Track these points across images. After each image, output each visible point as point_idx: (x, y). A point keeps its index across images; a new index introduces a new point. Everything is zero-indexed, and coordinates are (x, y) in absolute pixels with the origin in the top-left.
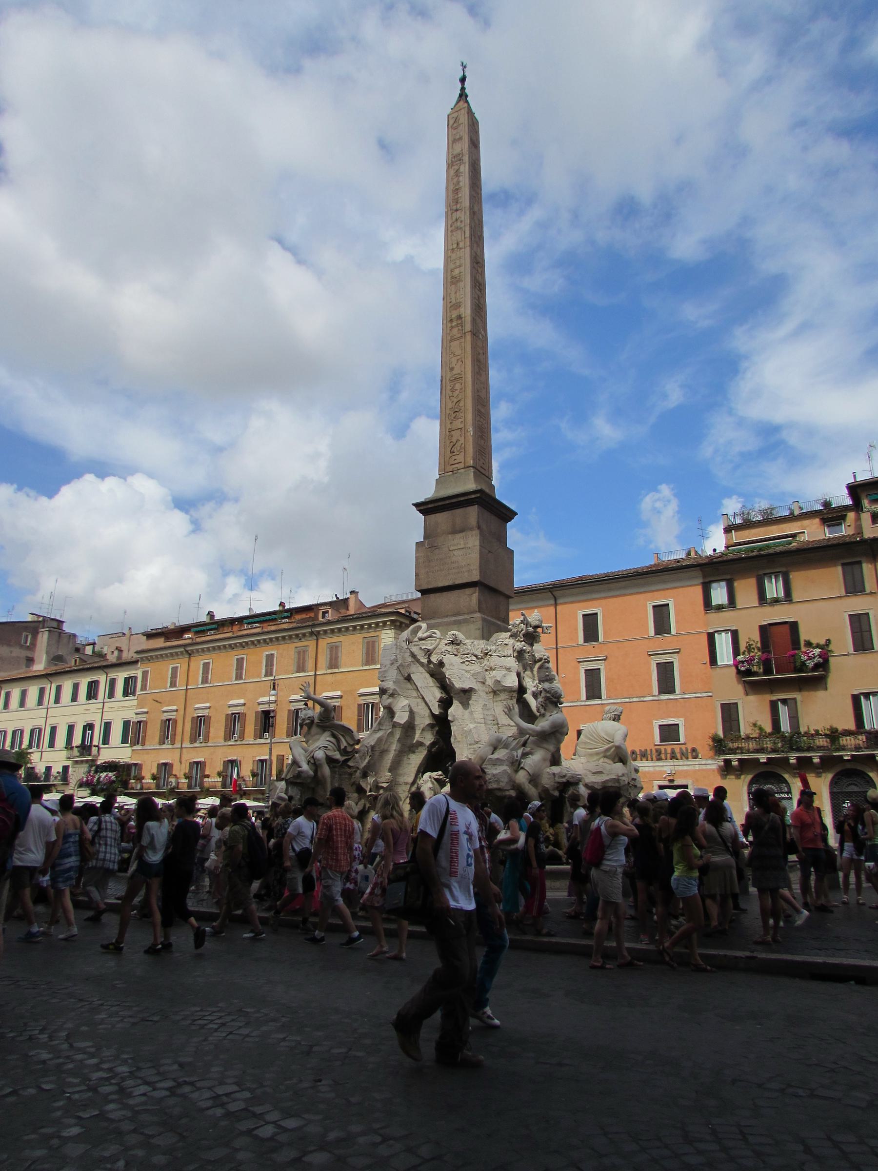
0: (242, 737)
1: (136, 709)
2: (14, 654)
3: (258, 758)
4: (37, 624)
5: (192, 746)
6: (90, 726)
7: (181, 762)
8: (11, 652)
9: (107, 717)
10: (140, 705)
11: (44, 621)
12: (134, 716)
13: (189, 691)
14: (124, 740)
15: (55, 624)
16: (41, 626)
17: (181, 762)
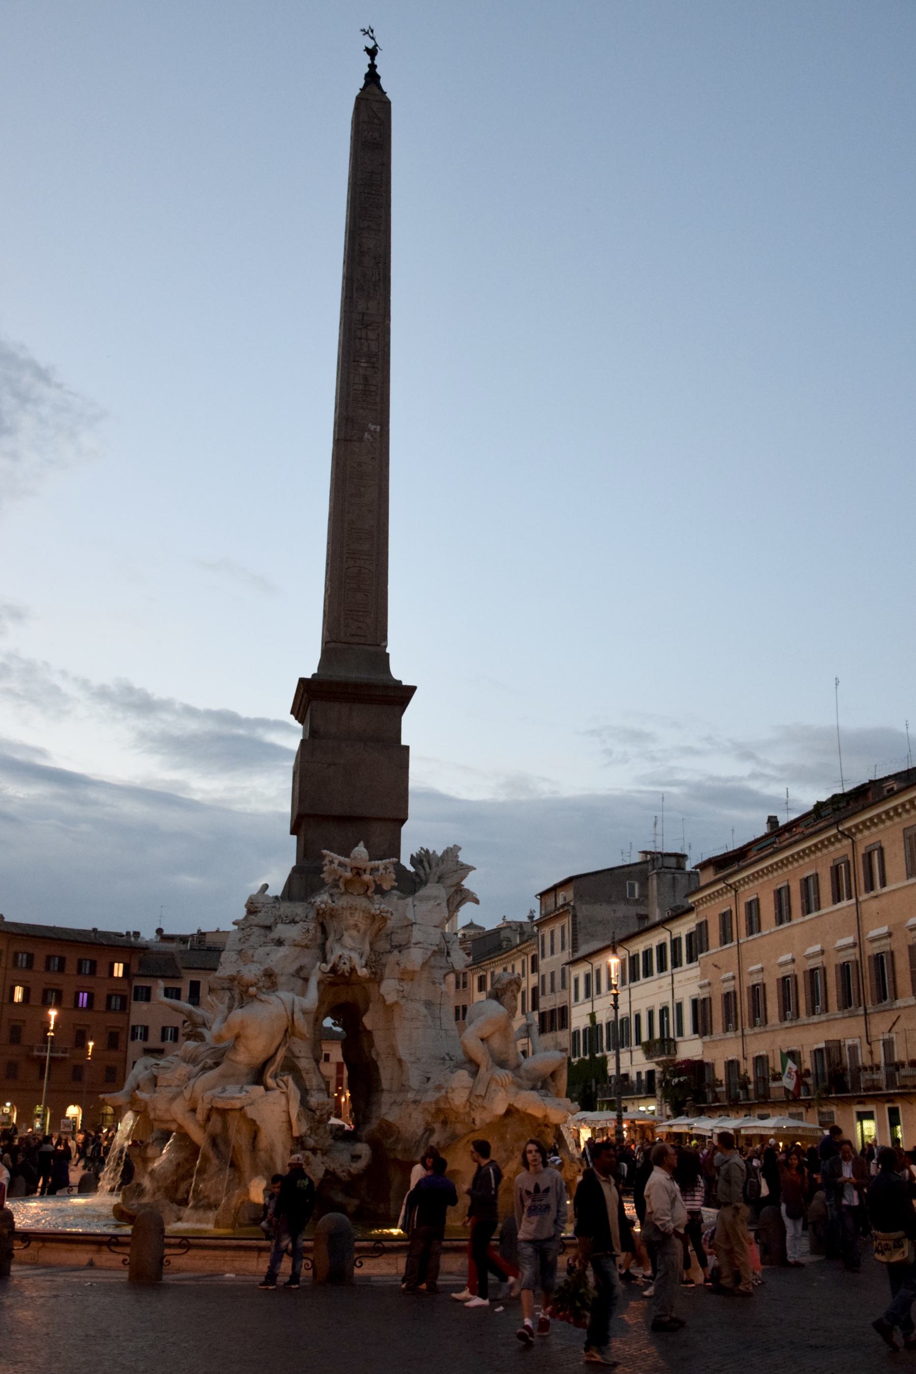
0: (797, 1015)
1: (700, 980)
2: (619, 914)
3: (816, 1047)
4: (644, 866)
5: (752, 1032)
6: (664, 1011)
7: (745, 1059)
8: (614, 911)
9: (677, 997)
10: (703, 975)
11: (653, 860)
12: (698, 991)
13: (743, 947)
14: (696, 1031)
15: (672, 862)
16: (650, 868)
17: (745, 1059)
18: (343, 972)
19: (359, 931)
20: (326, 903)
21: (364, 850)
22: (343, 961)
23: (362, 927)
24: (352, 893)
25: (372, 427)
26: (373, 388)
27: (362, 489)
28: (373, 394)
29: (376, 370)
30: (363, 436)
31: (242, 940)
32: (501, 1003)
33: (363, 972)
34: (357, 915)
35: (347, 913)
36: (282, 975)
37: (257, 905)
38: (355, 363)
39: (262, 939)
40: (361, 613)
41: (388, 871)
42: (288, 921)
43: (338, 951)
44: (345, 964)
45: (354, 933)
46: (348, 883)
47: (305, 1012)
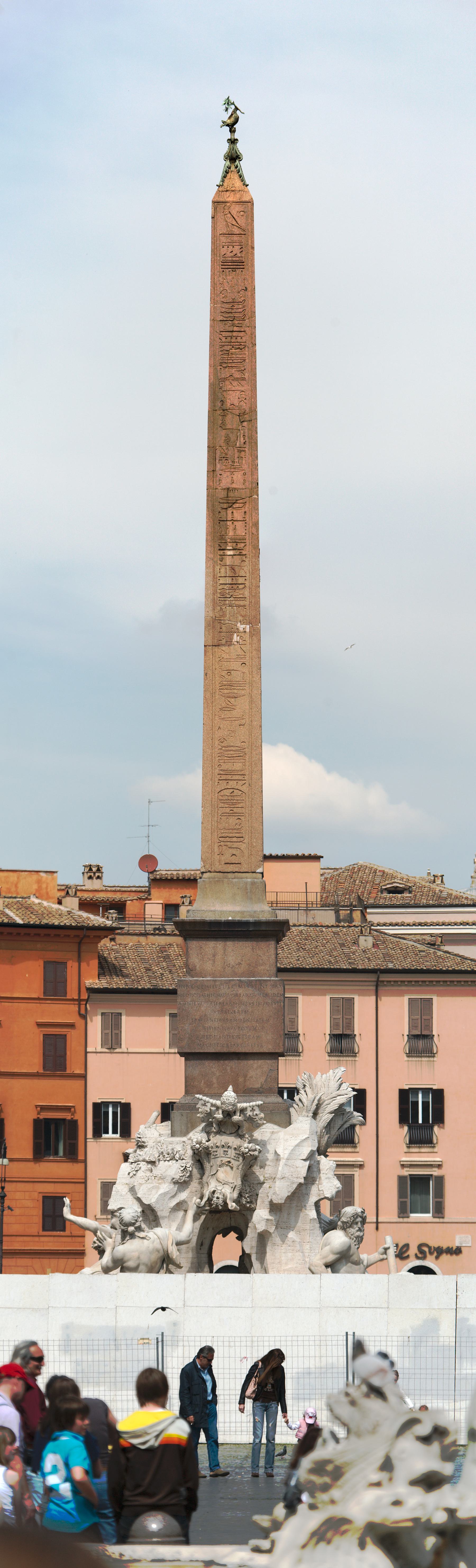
18: (217, 1206)
19: (232, 1168)
20: (200, 1143)
21: (233, 1094)
22: (216, 1195)
23: (235, 1163)
24: (224, 1133)
25: (241, 627)
26: (241, 580)
27: (232, 700)
28: (241, 586)
29: (244, 558)
30: (232, 639)
31: (131, 1174)
32: (347, 1234)
33: (232, 1205)
34: (229, 1152)
35: (220, 1151)
36: (162, 1210)
37: (143, 1140)
38: (221, 552)
39: (148, 1174)
40: (235, 839)
41: (255, 1113)
42: (168, 1159)
43: (213, 1185)
44: (218, 1198)
45: (228, 1168)
46: (220, 1123)
47: (178, 1244)
